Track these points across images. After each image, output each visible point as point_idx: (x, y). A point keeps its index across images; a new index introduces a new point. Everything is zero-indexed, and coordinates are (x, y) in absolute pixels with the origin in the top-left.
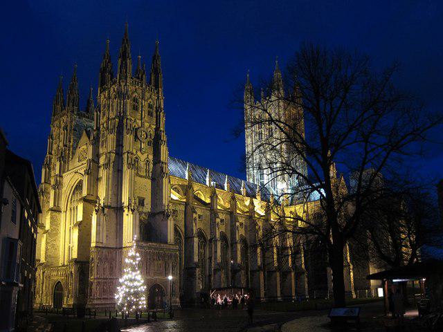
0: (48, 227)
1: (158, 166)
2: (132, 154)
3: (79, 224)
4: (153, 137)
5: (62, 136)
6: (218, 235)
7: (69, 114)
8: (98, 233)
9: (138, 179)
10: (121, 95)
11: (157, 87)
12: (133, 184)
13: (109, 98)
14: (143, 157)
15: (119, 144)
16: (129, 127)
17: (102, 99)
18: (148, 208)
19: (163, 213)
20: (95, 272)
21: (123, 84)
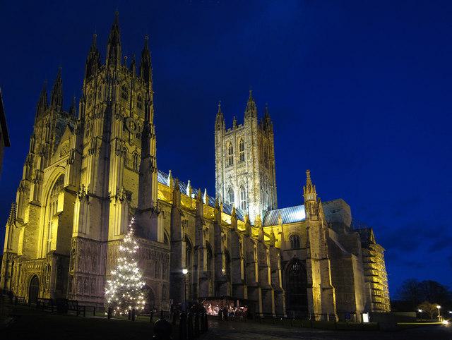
0: (26, 220)
1: (146, 160)
3: (60, 215)
5: (44, 135)
8: (81, 222)
9: (125, 170)
14: (131, 149)
18: (135, 203)
19: (152, 209)
20: (76, 265)
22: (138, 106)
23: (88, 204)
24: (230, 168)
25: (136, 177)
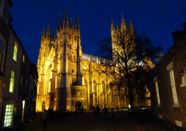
2: (69, 54)
3: (51, 80)
4: (76, 48)
5: (45, 48)
9: (71, 63)
10: (65, 34)
11: (77, 29)
12: (69, 65)
13: (61, 34)
14: (73, 55)
15: (65, 51)
16: (68, 45)
19: (80, 75)
25: (75, 64)
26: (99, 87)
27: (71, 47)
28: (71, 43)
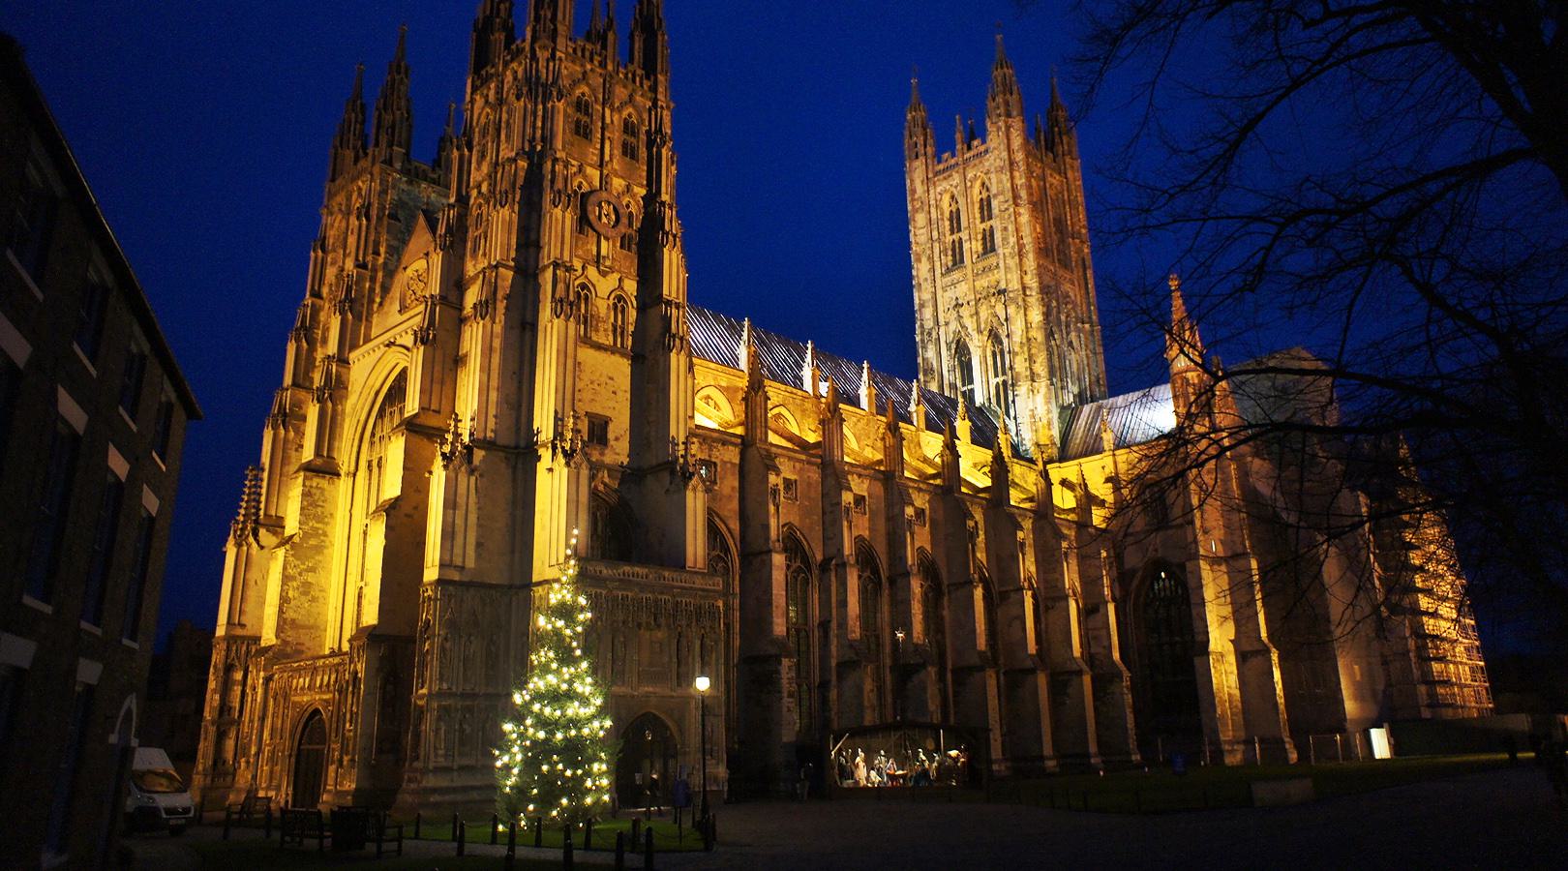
0: (292, 526)
1: (652, 312)
2: (570, 269)
3: (391, 509)
4: (637, 225)
5: (352, 240)
6: (848, 548)
7: (376, 170)
8: (448, 534)
9: (586, 354)
10: (537, 89)
11: (650, 70)
12: (570, 368)
13: (501, 101)
15: (529, 239)
16: (560, 185)
17: (479, 109)
18: (619, 451)
19: (670, 466)
20: (433, 670)
21: (542, 55)
22: (625, 153)
23: (472, 472)
24: (956, 275)
25: (620, 369)
26: (825, 590)
27: (593, 212)
28: (594, 174)
